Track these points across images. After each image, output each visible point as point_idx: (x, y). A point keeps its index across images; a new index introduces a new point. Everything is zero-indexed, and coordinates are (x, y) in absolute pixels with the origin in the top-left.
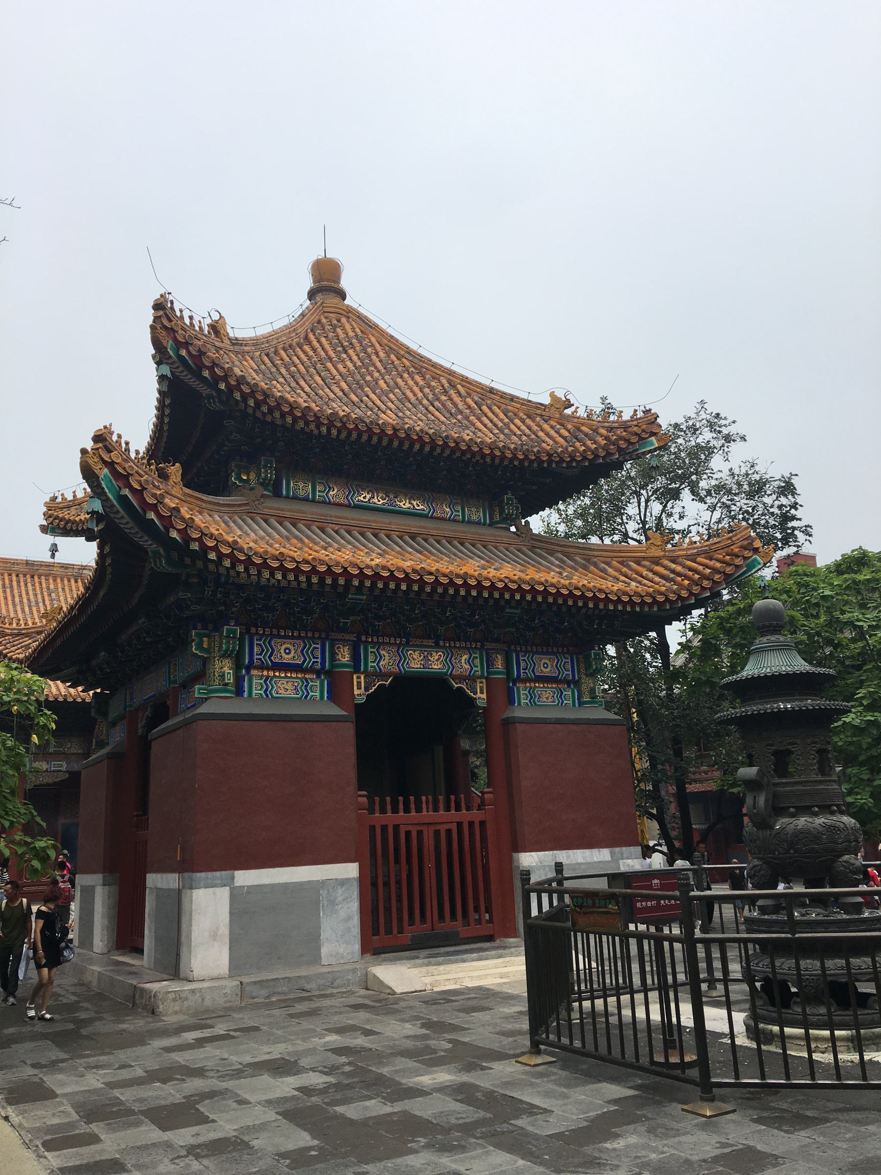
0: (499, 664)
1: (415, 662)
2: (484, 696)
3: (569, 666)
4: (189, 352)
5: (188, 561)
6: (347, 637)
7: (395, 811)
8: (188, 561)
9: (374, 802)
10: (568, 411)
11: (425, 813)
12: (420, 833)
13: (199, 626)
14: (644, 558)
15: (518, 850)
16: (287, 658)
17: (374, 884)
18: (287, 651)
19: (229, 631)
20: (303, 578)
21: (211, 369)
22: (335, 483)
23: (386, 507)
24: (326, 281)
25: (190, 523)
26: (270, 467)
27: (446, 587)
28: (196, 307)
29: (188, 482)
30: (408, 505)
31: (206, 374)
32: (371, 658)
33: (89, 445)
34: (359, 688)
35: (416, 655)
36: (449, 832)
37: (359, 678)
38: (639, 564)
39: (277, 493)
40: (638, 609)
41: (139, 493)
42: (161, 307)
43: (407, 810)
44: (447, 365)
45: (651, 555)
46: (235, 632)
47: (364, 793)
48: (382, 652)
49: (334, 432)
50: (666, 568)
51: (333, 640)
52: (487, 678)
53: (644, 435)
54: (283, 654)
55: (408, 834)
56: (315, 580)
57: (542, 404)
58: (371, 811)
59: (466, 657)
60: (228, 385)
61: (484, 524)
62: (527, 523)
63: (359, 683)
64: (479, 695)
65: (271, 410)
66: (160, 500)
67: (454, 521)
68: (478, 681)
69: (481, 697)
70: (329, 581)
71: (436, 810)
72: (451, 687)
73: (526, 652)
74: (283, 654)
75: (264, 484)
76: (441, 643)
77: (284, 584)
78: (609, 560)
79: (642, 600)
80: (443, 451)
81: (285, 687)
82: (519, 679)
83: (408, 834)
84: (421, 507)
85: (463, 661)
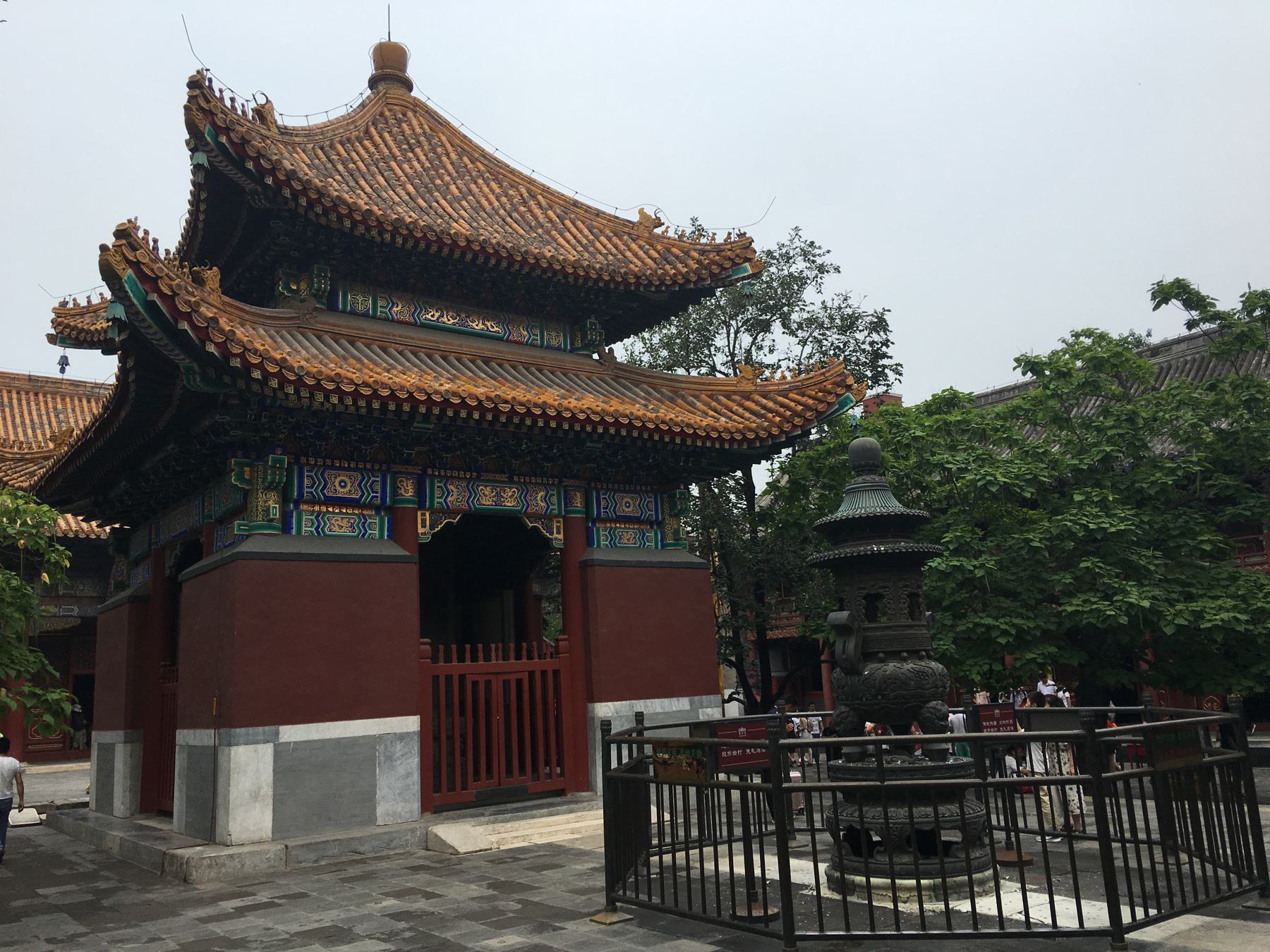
0: (578, 502)
1: (486, 498)
2: (561, 536)
3: (652, 506)
4: (229, 139)
5: (227, 379)
6: (410, 469)
7: (461, 659)
8: (227, 379)
9: (438, 650)
10: (658, 231)
12: (488, 683)
13: (240, 453)
14: (735, 392)
15: (593, 700)
16: (342, 492)
17: (437, 739)
18: (343, 485)
19: (275, 461)
20: (362, 403)
21: (256, 160)
22: (399, 298)
23: (457, 327)
24: (390, 67)
25: (230, 336)
26: (325, 277)
27: (522, 417)
28: (239, 87)
29: (227, 288)
30: (481, 326)
31: (250, 165)
32: (437, 493)
33: (110, 241)
34: (424, 526)
35: (488, 491)
36: (519, 682)
37: (423, 515)
38: (728, 398)
39: (332, 307)
40: (727, 446)
41: (170, 299)
42: (199, 85)
44: (527, 172)
46: (281, 462)
48: (451, 487)
49: (399, 240)
50: (757, 403)
51: (396, 473)
52: (564, 517)
53: (737, 261)
54: (338, 488)
55: (475, 684)
56: (376, 405)
58: (435, 659)
61: (565, 350)
62: (611, 350)
63: (424, 521)
64: (555, 535)
65: (326, 211)
66: (195, 308)
67: (533, 345)
69: (558, 537)
70: (392, 407)
72: (525, 526)
73: (607, 489)
74: (338, 488)
75: (317, 296)
76: (516, 479)
77: (340, 409)
80: (521, 267)
81: (340, 524)
82: (599, 519)
83: (475, 684)
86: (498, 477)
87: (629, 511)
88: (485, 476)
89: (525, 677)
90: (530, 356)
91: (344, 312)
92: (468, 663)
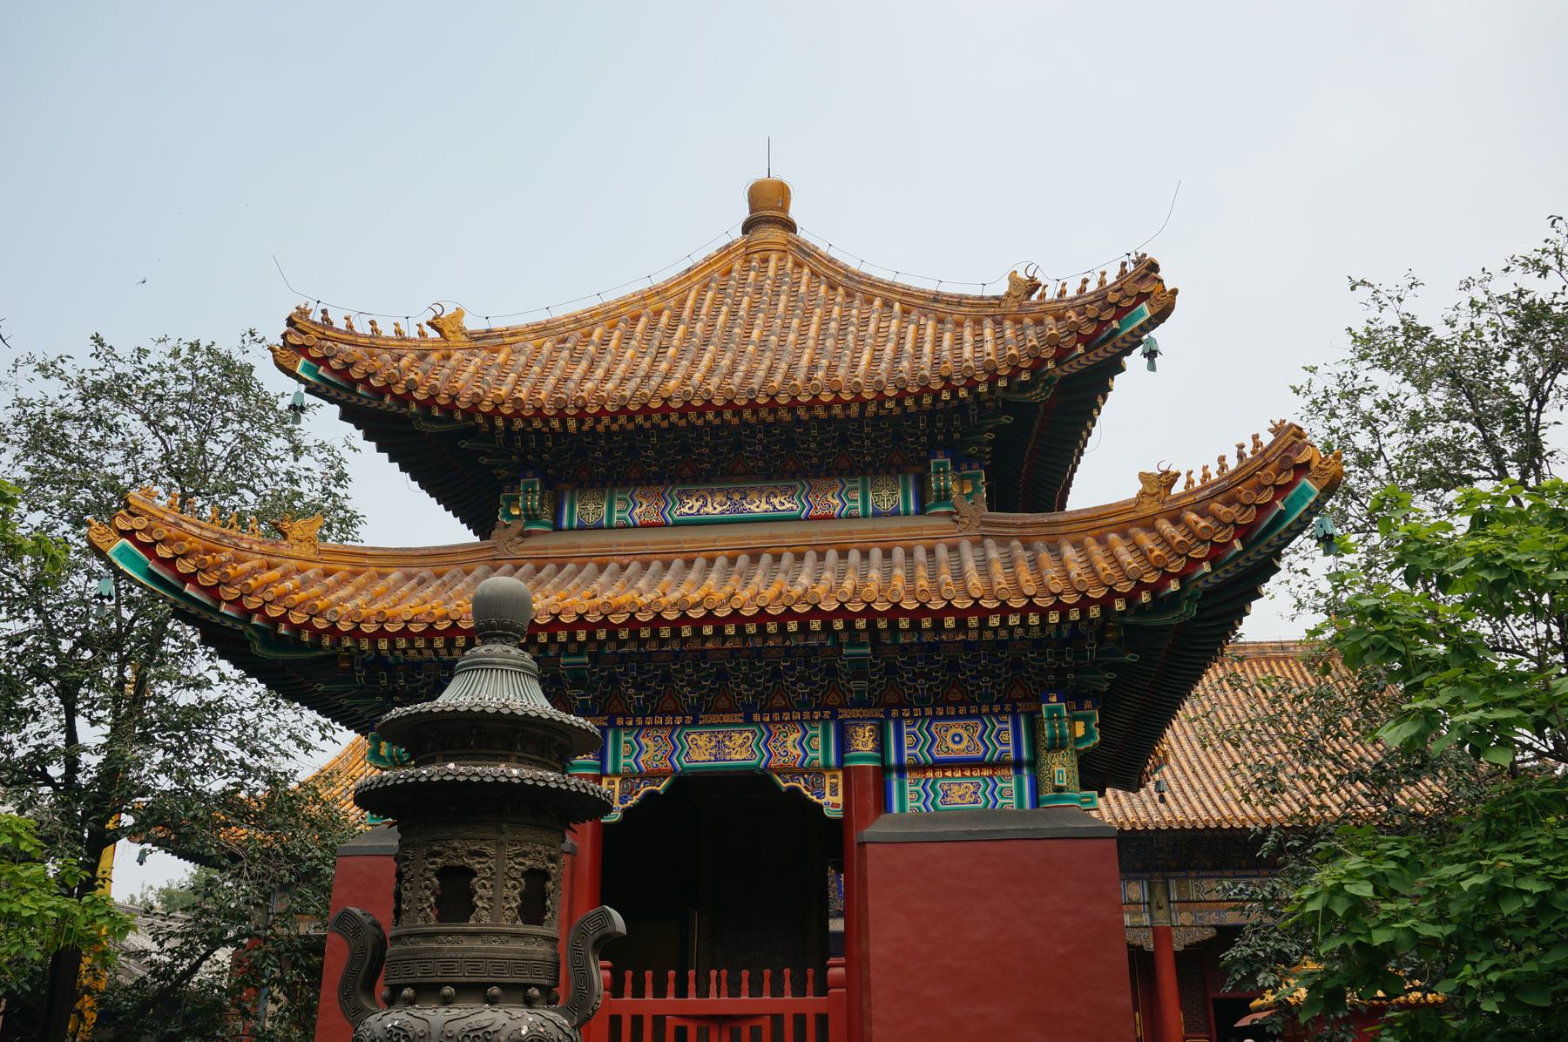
0: (864, 741)
1: (701, 751)
2: (839, 799)
3: (1008, 737)
7: (660, 992)
11: (713, 997)
21: (365, 381)
22: (644, 496)
23: (727, 516)
24: (768, 210)
30: (764, 506)
32: (623, 749)
35: (702, 740)
39: (557, 528)
43: (682, 992)
45: (1142, 514)
47: (608, 963)
48: (643, 741)
49: (572, 424)
53: (1126, 303)
57: (996, 298)
59: (797, 736)
60: (394, 396)
61: (907, 513)
65: (918, 398)
67: (849, 517)
68: (827, 775)
69: (832, 801)
76: (756, 717)
78: (1081, 536)
79: (1058, 601)
82: (901, 770)
84: (788, 505)
86: (727, 718)
87: (959, 750)
88: (704, 719)
89: (766, 1024)
90: (829, 534)
91: (571, 529)
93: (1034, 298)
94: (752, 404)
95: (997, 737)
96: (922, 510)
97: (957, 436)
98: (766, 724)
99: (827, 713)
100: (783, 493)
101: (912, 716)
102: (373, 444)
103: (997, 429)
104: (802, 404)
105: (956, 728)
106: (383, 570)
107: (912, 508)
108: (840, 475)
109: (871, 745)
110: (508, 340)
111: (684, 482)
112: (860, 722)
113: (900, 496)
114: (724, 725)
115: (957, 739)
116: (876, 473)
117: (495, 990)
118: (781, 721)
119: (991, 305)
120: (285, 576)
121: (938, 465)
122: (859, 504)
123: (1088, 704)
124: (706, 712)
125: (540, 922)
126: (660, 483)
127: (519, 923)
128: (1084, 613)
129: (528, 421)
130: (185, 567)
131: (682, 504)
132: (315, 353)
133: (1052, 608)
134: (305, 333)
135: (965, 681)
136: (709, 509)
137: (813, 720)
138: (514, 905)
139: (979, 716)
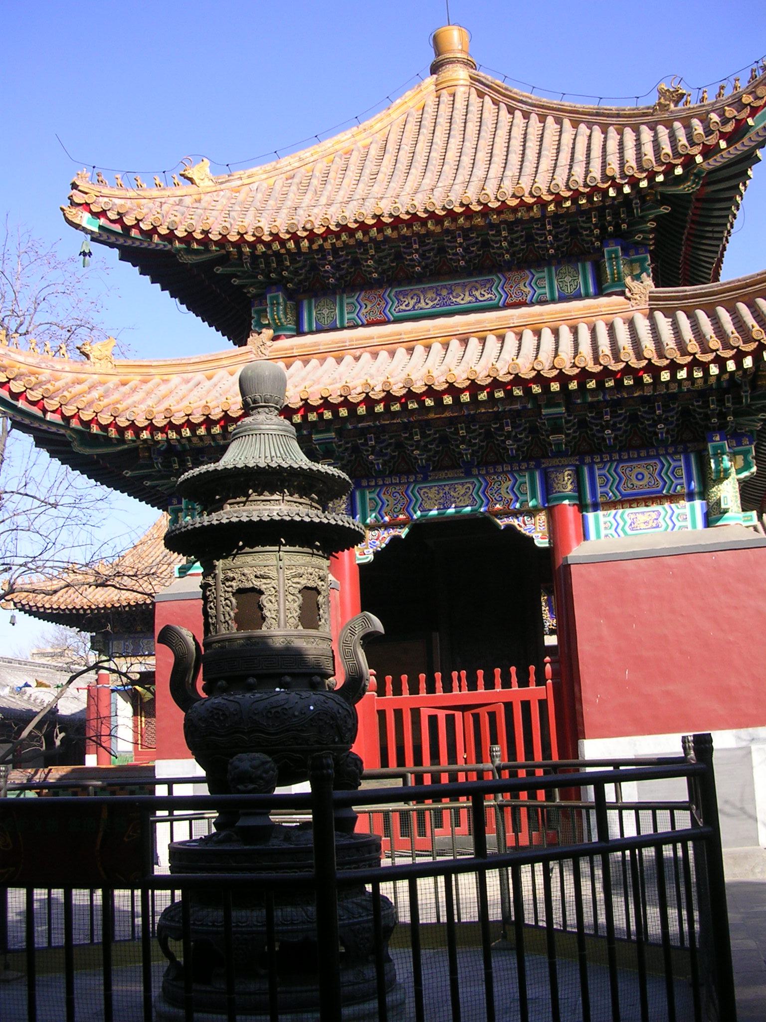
11: (456, 692)
13: (175, 501)
21: (137, 226)
30: (468, 298)
36: (492, 716)
48: (384, 497)
49: (305, 244)
55: (433, 719)
57: (648, 108)
59: (510, 483)
61: (587, 296)
71: (473, 686)
72: (497, 526)
83: (433, 719)
84: (487, 296)
85: (503, 491)
92: (515, 688)
93: (680, 106)
94: (451, 213)
95: (672, 473)
96: (600, 292)
97: (624, 226)
98: (483, 476)
99: (532, 464)
100: (483, 285)
101: (602, 461)
102: (148, 277)
103: (658, 219)
104: (492, 209)
105: (639, 467)
106: (166, 377)
107: (591, 290)
108: (529, 268)
109: (570, 487)
110: (247, 181)
111: (400, 284)
112: (560, 468)
113: (581, 280)
114: (449, 479)
115: (640, 477)
116: (559, 263)
117: (288, 679)
118: (495, 473)
119: (645, 115)
120: (92, 388)
121: (610, 252)
122: (547, 290)
123: (746, 441)
124: (434, 470)
125: (316, 627)
126: (381, 287)
127: (300, 627)
128: (739, 364)
129: (268, 245)
130: (16, 387)
131: (400, 302)
132: (95, 209)
133: (712, 362)
134: (86, 193)
135: (644, 429)
136: (423, 304)
137: (520, 470)
138: (295, 615)
139: (657, 457)
